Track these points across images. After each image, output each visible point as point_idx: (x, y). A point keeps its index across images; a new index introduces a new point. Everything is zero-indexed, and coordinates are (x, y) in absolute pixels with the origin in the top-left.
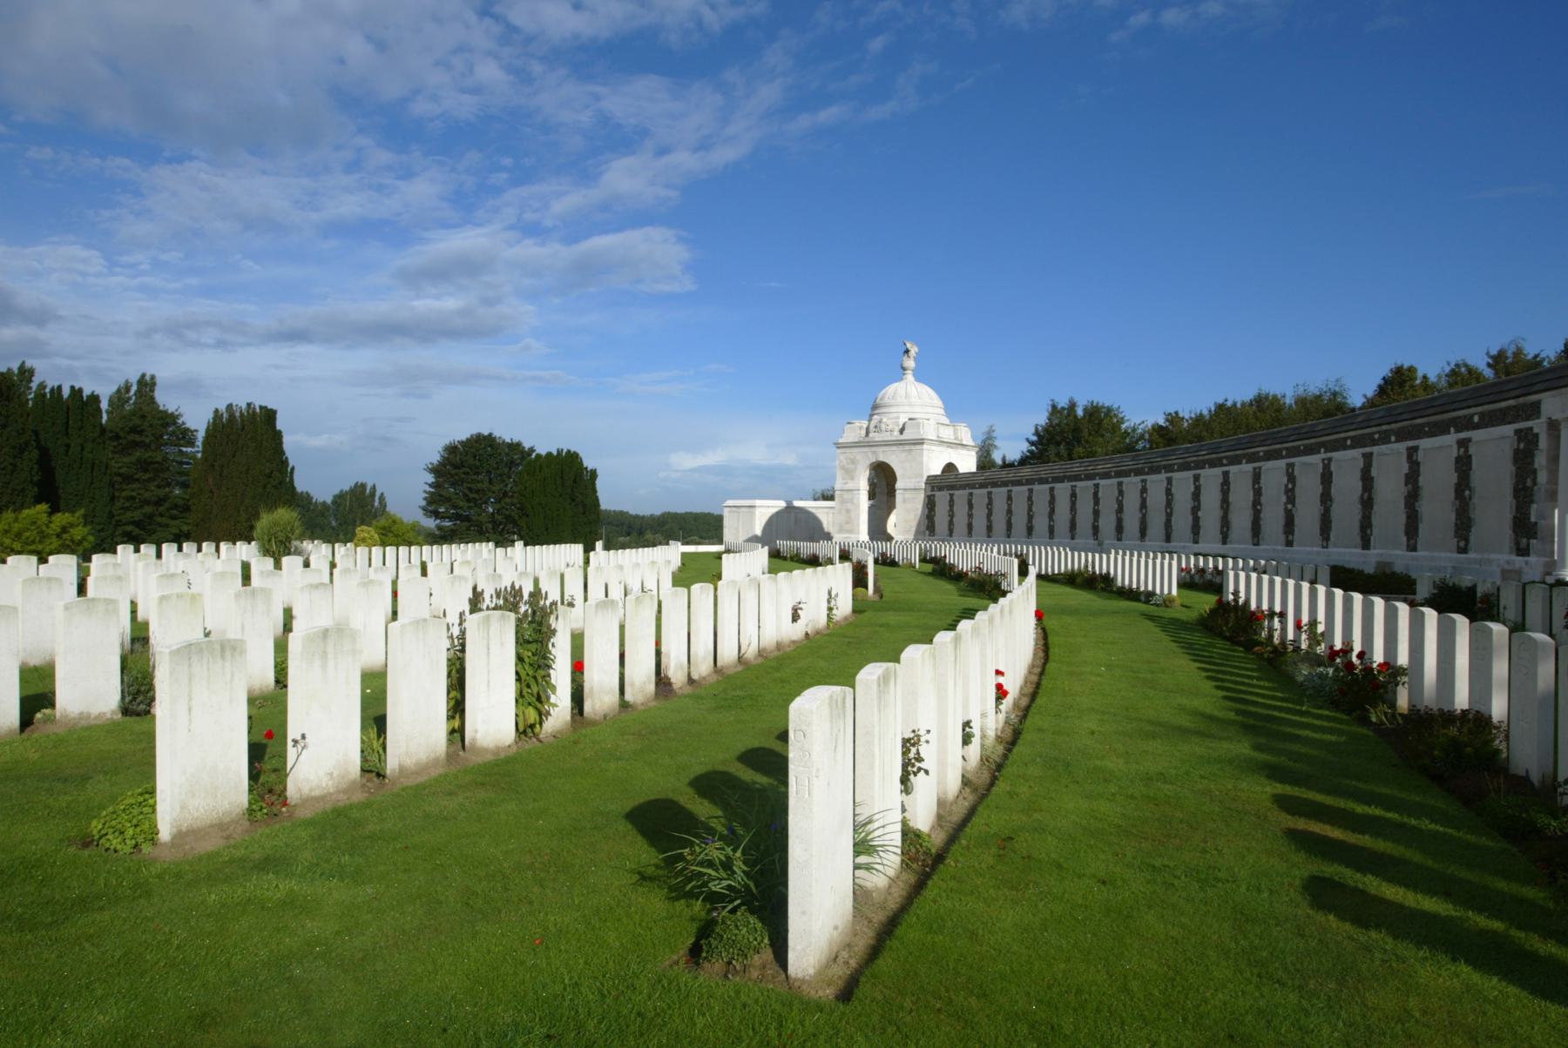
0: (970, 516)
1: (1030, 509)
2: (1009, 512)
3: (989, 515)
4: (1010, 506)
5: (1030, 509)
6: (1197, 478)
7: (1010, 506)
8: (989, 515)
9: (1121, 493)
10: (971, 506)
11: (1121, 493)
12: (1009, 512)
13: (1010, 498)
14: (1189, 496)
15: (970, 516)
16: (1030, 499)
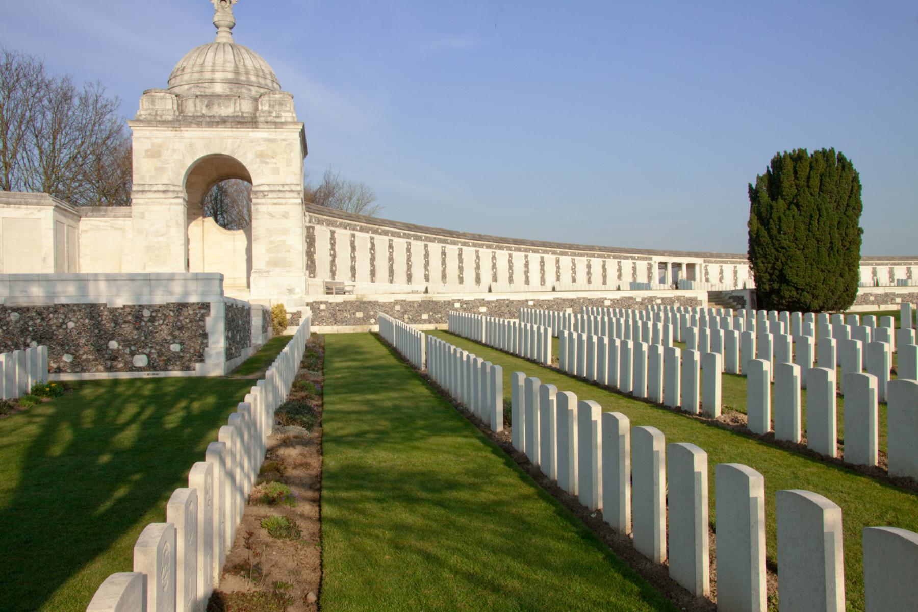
0: (353, 258)
1: (409, 259)
2: (391, 259)
3: (373, 259)
4: (391, 254)
5: (409, 259)
6: (526, 257)
7: (391, 254)
8: (373, 259)
9: (478, 257)
10: (353, 249)
11: (478, 257)
12: (391, 259)
13: (391, 247)
14: (523, 266)
15: (353, 258)
16: (408, 250)
